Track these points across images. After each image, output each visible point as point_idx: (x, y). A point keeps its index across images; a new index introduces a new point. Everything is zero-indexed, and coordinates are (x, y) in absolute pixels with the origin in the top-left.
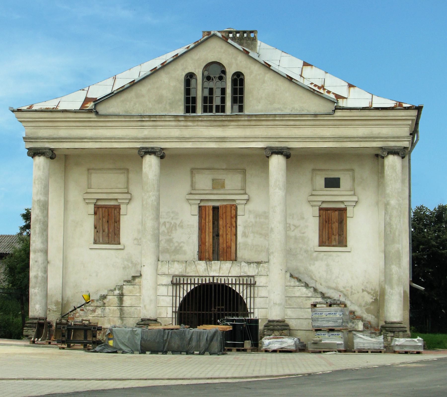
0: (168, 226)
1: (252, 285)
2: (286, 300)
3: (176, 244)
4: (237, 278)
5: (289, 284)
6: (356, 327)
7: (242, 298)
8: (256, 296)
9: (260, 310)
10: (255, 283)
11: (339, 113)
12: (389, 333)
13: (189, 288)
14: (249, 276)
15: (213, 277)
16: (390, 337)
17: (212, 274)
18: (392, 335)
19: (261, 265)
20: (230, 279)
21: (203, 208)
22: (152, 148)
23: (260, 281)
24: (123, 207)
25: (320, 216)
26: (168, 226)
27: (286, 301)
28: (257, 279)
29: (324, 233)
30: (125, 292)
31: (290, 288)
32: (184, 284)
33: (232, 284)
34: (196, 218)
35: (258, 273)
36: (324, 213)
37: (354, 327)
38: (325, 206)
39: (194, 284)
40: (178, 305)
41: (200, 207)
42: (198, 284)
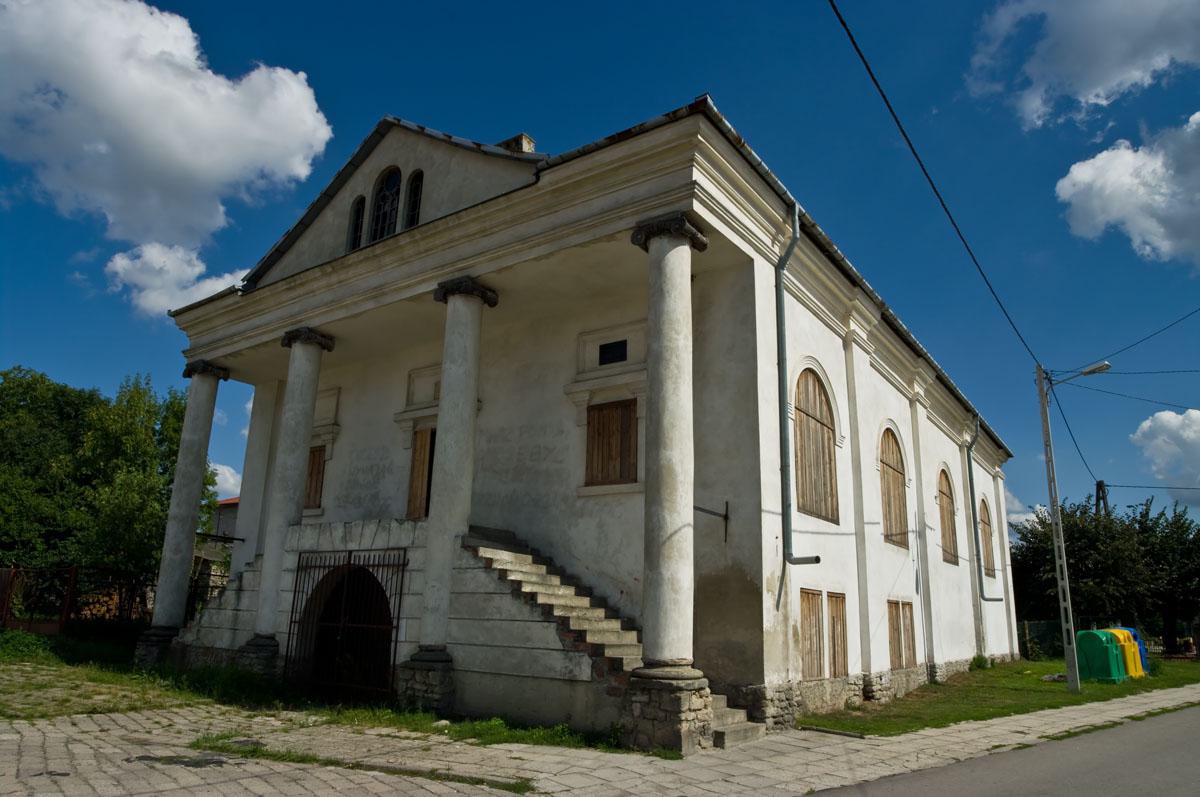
0: (374, 473)
1: (402, 566)
2: (451, 600)
3: (382, 502)
4: (382, 553)
5: (457, 563)
6: (576, 672)
7: (384, 592)
8: (405, 591)
9: (410, 621)
10: (405, 564)
11: (547, 178)
12: (638, 693)
13: (319, 575)
14: (399, 549)
15: (350, 552)
16: (638, 705)
17: (352, 546)
18: (645, 698)
19: (420, 524)
20: (372, 554)
21: (419, 435)
22: (297, 330)
23: (415, 558)
24: (328, 448)
25: (589, 423)
26: (374, 473)
27: (451, 603)
28: (410, 555)
29: (595, 457)
30: (245, 581)
31: (459, 573)
32: (311, 567)
33: (373, 566)
34: (410, 452)
35: (413, 543)
36: (596, 415)
37: (571, 671)
38: (598, 400)
39: (324, 567)
40: (299, 610)
41: (415, 433)
42: (329, 567)
